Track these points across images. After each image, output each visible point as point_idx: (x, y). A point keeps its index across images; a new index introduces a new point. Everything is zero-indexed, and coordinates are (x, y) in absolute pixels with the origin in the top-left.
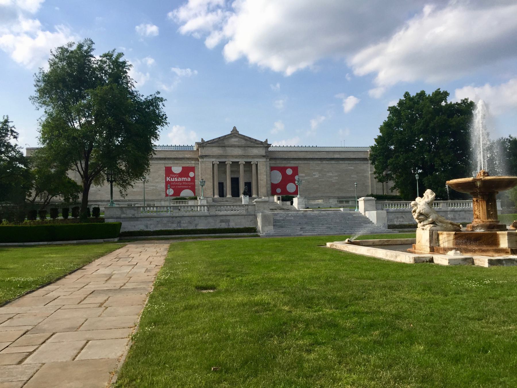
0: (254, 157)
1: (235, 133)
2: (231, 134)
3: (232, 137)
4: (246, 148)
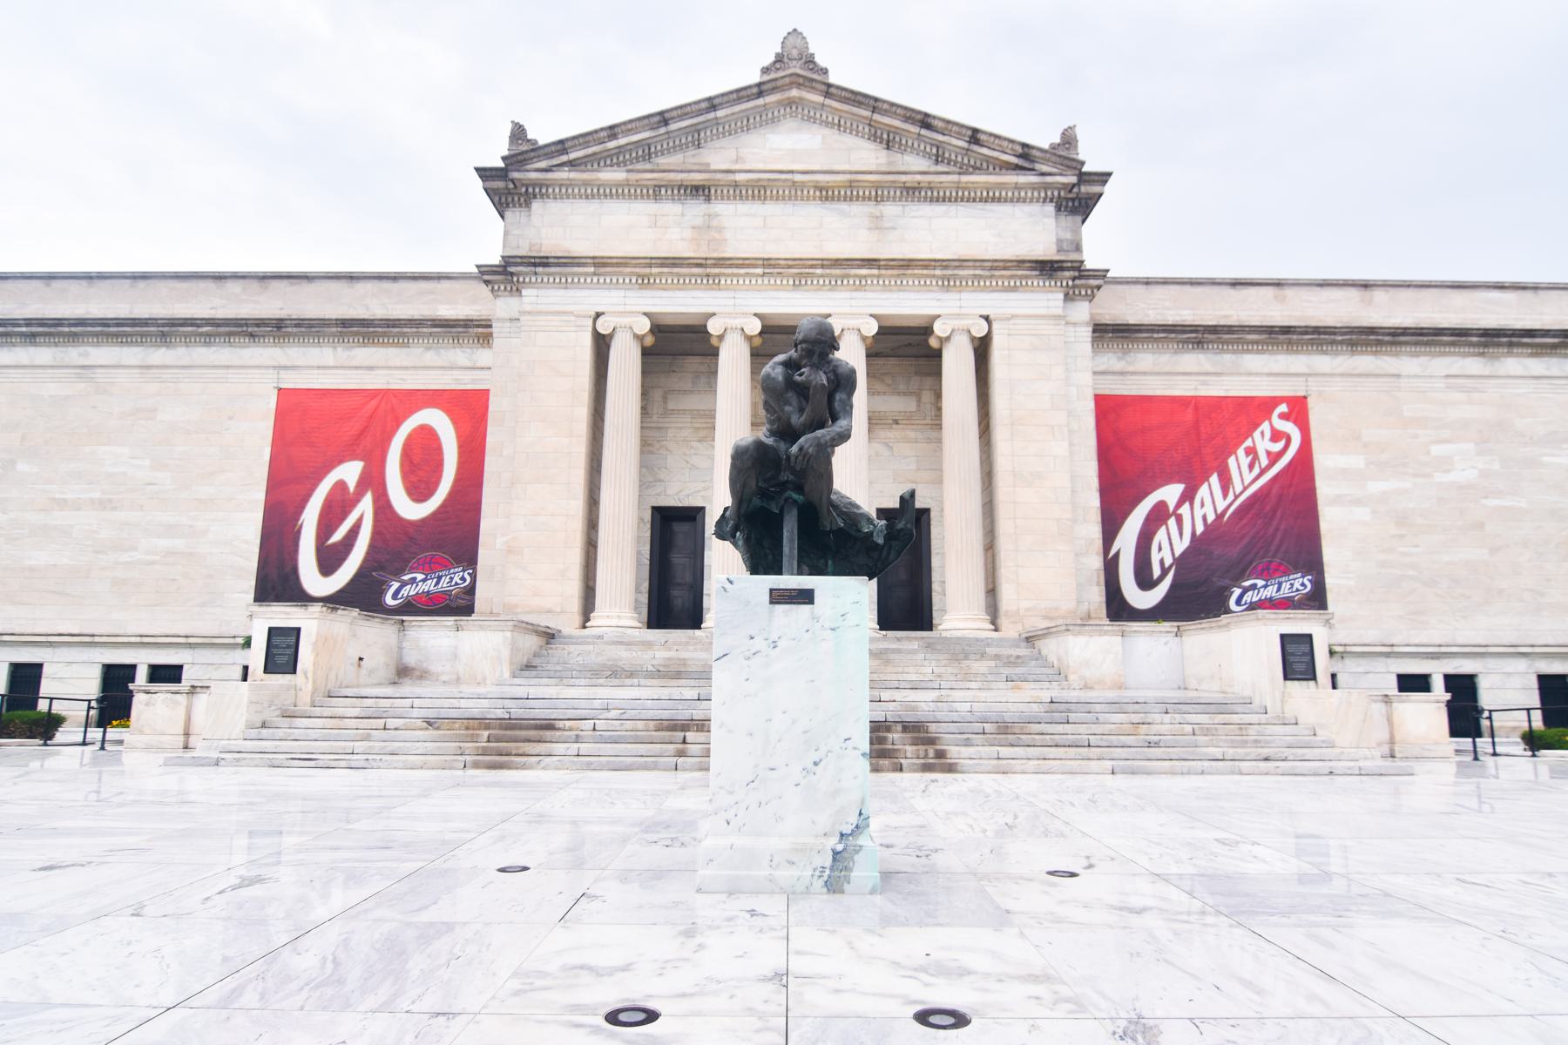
2: (760, 90)
3: (765, 119)
4: (890, 209)
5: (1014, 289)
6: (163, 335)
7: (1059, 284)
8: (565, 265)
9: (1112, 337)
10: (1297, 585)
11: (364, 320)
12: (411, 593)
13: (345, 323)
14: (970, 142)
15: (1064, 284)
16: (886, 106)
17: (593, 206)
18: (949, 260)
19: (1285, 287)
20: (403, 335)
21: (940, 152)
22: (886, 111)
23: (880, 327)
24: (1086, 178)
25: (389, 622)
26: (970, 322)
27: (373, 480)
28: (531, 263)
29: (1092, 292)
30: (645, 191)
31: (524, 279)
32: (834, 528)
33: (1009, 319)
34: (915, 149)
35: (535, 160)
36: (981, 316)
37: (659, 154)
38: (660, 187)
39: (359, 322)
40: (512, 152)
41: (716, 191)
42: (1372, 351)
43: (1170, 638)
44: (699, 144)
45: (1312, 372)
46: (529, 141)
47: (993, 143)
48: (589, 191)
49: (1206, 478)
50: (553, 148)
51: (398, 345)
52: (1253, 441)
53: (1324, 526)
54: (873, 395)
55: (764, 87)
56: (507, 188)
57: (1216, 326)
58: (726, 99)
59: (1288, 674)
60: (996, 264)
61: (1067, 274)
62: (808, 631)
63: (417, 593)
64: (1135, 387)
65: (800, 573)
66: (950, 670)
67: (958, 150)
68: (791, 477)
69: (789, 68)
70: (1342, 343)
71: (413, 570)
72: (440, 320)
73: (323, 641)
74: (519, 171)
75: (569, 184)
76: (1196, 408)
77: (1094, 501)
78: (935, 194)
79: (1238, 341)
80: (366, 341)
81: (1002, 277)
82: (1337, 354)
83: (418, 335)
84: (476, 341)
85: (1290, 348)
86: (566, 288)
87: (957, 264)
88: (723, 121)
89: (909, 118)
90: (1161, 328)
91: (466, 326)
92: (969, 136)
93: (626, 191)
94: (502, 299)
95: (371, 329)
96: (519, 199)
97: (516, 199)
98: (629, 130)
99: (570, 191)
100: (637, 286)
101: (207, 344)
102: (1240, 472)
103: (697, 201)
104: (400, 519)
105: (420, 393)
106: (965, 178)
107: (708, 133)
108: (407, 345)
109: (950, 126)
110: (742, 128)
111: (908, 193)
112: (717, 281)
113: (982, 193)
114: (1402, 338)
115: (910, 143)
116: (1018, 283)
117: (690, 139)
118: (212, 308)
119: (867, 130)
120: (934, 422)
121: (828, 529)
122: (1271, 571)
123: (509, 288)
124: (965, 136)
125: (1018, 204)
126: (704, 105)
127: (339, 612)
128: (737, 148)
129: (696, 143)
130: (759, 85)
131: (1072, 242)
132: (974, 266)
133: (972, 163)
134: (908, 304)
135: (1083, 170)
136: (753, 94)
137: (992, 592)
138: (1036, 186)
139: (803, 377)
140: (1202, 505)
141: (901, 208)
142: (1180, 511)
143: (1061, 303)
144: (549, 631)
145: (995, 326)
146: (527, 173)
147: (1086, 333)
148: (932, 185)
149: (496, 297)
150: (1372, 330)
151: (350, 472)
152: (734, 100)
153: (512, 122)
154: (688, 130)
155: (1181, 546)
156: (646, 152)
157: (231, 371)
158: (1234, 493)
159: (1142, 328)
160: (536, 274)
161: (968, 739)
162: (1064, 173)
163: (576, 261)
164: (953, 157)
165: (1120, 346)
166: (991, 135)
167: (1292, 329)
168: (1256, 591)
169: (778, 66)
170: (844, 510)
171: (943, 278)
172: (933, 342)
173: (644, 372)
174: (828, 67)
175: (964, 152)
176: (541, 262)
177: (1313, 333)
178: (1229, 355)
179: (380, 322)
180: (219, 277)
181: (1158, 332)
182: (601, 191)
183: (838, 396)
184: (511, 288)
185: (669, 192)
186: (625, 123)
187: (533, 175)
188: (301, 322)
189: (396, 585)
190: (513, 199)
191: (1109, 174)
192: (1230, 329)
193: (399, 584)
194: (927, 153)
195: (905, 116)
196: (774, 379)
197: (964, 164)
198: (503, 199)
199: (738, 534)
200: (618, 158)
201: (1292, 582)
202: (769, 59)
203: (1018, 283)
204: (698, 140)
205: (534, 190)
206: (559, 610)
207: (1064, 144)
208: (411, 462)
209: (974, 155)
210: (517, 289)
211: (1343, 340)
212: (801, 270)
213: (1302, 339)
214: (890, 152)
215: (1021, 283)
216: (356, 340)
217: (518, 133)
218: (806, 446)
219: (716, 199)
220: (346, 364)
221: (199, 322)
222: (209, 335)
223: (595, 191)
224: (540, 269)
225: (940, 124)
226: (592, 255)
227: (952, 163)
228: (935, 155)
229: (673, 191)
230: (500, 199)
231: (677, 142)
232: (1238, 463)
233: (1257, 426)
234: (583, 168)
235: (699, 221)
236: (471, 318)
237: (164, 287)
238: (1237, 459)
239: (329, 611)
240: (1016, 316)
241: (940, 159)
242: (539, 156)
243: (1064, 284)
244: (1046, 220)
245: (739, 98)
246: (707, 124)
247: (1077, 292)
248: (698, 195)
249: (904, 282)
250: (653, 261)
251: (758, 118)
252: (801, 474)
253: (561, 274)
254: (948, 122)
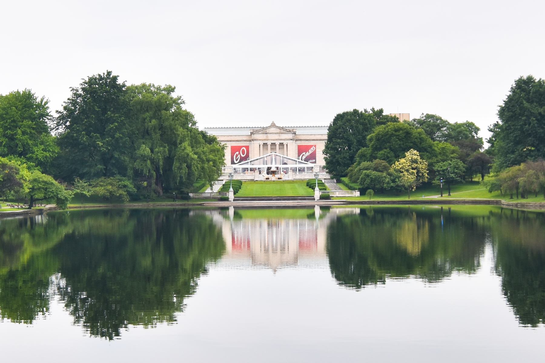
0: (284, 140)
1: (273, 125)
4: (280, 134)
27: (239, 153)
134: (281, 142)
151: (237, 153)
155: (305, 158)
212: (274, 140)
232: (310, 151)
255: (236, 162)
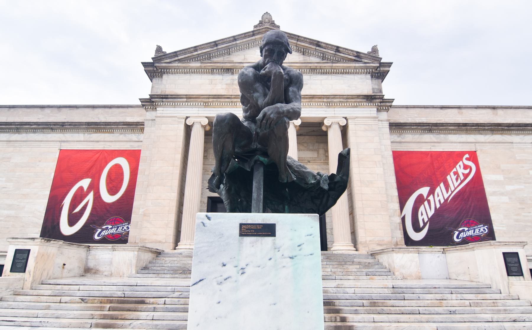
2: (253, 33)
5: (356, 107)
6: (17, 129)
7: (374, 105)
8: (175, 98)
9: (395, 128)
10: (482, 230)
11: (96, 123)
12: (106, 234)
13: (88, 124)
14: (336, 52)
15: (377, 104)
16: (302, 39)
17: (187, 76)
18: (329, 95)
19: (462, 109)
20: (111, 128)
21: (324, 56)
22: (302, 40)
23: (302, 122)
24: (383, 65)
25: (82, 247)
26: (339, 120)
27: (94, 187)
28: (161, 97)
29: (388, 108)
30: (208, 70)
31: (158, 104)
32: (290, 181)
33: (355, 118)
34: (314, 55)
35: (165, 59)
36: (343, 117)
37: (214, 57)
38: (214, 69)
39: (94, 123)
40: (156, 56)
41: (236, 70)
42: (500, 133)
43: (440, 254)
44: (229, 54)
45: (477, 142)
46: (163, 52)
47: (345, 52)
48: (186, 71)
49: (439, 185)
50: (172, 55)
51: (109, 133)
52: (457, 169)
53: (490, 204)
54: (299, 151)
55: (255, 32)
56: (153, 70)
57: (437, 123)
58: (240, 37)
59: (510, 273)
60: (349, 97)
61: (378, 100)
62: (270, 259)
63: (108, 234)
64: (405, 148)
65: (264, 211)
66: (339, 270)
67: (331, 55)
68: (259, 146)
69: (265, 26)
70: (488, 130)
71: (107, 224)
72: (126, 123)
73: (41, 256)
74: (158, 63)
75: (178, 68)
76: (431, 156)
77: (395, 193)
78: (323, 71)
79: (446, 130)
80: (97, 131)
81: (351, 102)
82: (486, 134)
83: (118, 129)
84: (140, 131)
85: (467, 132)
86: (175, 107)
87: (333, 97)
88: (239, 45)
89: (312, 43)
90: (414, 124)
91: (136, 125)
92: (335, 50)
93: (200, 71)
94: (149, 112)
95: (99, 126)
96: (158, 75)
97: (157, 74)
98: (202, 48)
99: (178, 71)
100: (203, 106)
101: (34, 132)
102: (453, 182)
103: (228, 74)
104: (108, 204)
105: (117, 151)
106: (334, 65)
107: (233, 49)
108: (113, 133)
109: (328, 46)
110: (246, 47)
111: (312, 71)
112: (235, 104)
113: (341, 70)
114: (512, 128)
115: (312, 52)
116: (358, 104)
117: (226, 51)
118: (38, 119)
119: (295, 48)
120: (324, 162)
121: (285, 181)
122: (470, 224)
123: (152, 108)
124: (334, 49)
125: (355, 75)
126: (231, 39)
127: (52, 242)
128: (244, 55)
129: (229, 53)
130: (253, 31)
131: (378, 89)
132: (339, 98)
133: (337, 59)
135: (381, 62)
136: (251, 35)
137: (354, 233)
138: (362, 68)
139: (267, 70)
140: (438, 196)
141: (309, 76)
142: (429, 198)
143: (376, 112)
144: (158, 251)
145: (349, 121)
146: (161, 64)
147: (387, 125)
148: (322, 67)
149: (147, 111)
150: (499, 125)
151: (85, 183)
152: (243, 37)
153: (157, 45)
154: (225, 48)
155: (431, 213)
156: (208, 57)
157: (42, 143)
158: (451, 191)
159: (407, 124)
160: (163, 102)
161: (356, 310)
162: (374, 62)
163: (179, 96)
164: (329, 57)
165: (398, 132)
166: (344, 49)
167: (467, 125)
168: (465, 233)
169: (260, 25)
170: (296, 169)
171: (327, 102)
172: (324, 128)
173: (205, 142)
174: (280, 26)
175: (334, 55)
176: (164, 97)
177: (476, 126)
178: (443, 135)
179: (102, 123)
180: (42, 107)
181: (413, 126)
182: (191, 71)
183: (291, 89)
184: (153, 107)
185: (217, 71)
186: (201, 45)
187: (164, 65)
188: (72, 123)
189: (99, 230)
190: (156, 74)
191: (392, 63)
192: (442, 125)
193: (101, 230)
194: (319, 56)
195: (310, 42)
196: (246, 75)
197: (334, 60)
198: (152, 75)
199: (222, 186)
200: (198, 59)
201: (480, 228)
202: (257, 22)
203: (358, 104)
204: (229, 52)
205: (164, 70)
206: (164, 241)
207: (373, 52)
208: (110, 179)
209: (338, 56)
210: (155, 108)
211: (488, 129)
213: (472, 129)
214: (304, 56)
215: (359, 104)
216: (93, 131)
217: (159, 49)
218: (269, 113)
219: (236, 73)
220: (89, 140)
221: (32, 124)
222: (35, 129)
223: (188, 70)
224: (164, 100)
225: (324, 45)
226: (185, 94)
227: (329, 60)
228: (322, 57)
229: (219, 71)
230: (151, 74)
231: (221, 53)
232: (451, 178)
233: (457, 163)
234: (184, 62)
235: (229, 82)
236: (139, 122)
237: (20, 111)
238: (451, 177)
239: (46, 241)
240: (358, 117)
241: (324, 58)
242: (166, 58)
243: (377, 104)
244: (367, 81)
245: (245, 36)
246: (233, 46)
247: (382, 108)
248: (228, 72)
249: (312, 104)
250: (210, 96)
251: (252, 44)
252: (264, 140)
253: (173, 102)
254: (327, 44)
255: (66, 229)
